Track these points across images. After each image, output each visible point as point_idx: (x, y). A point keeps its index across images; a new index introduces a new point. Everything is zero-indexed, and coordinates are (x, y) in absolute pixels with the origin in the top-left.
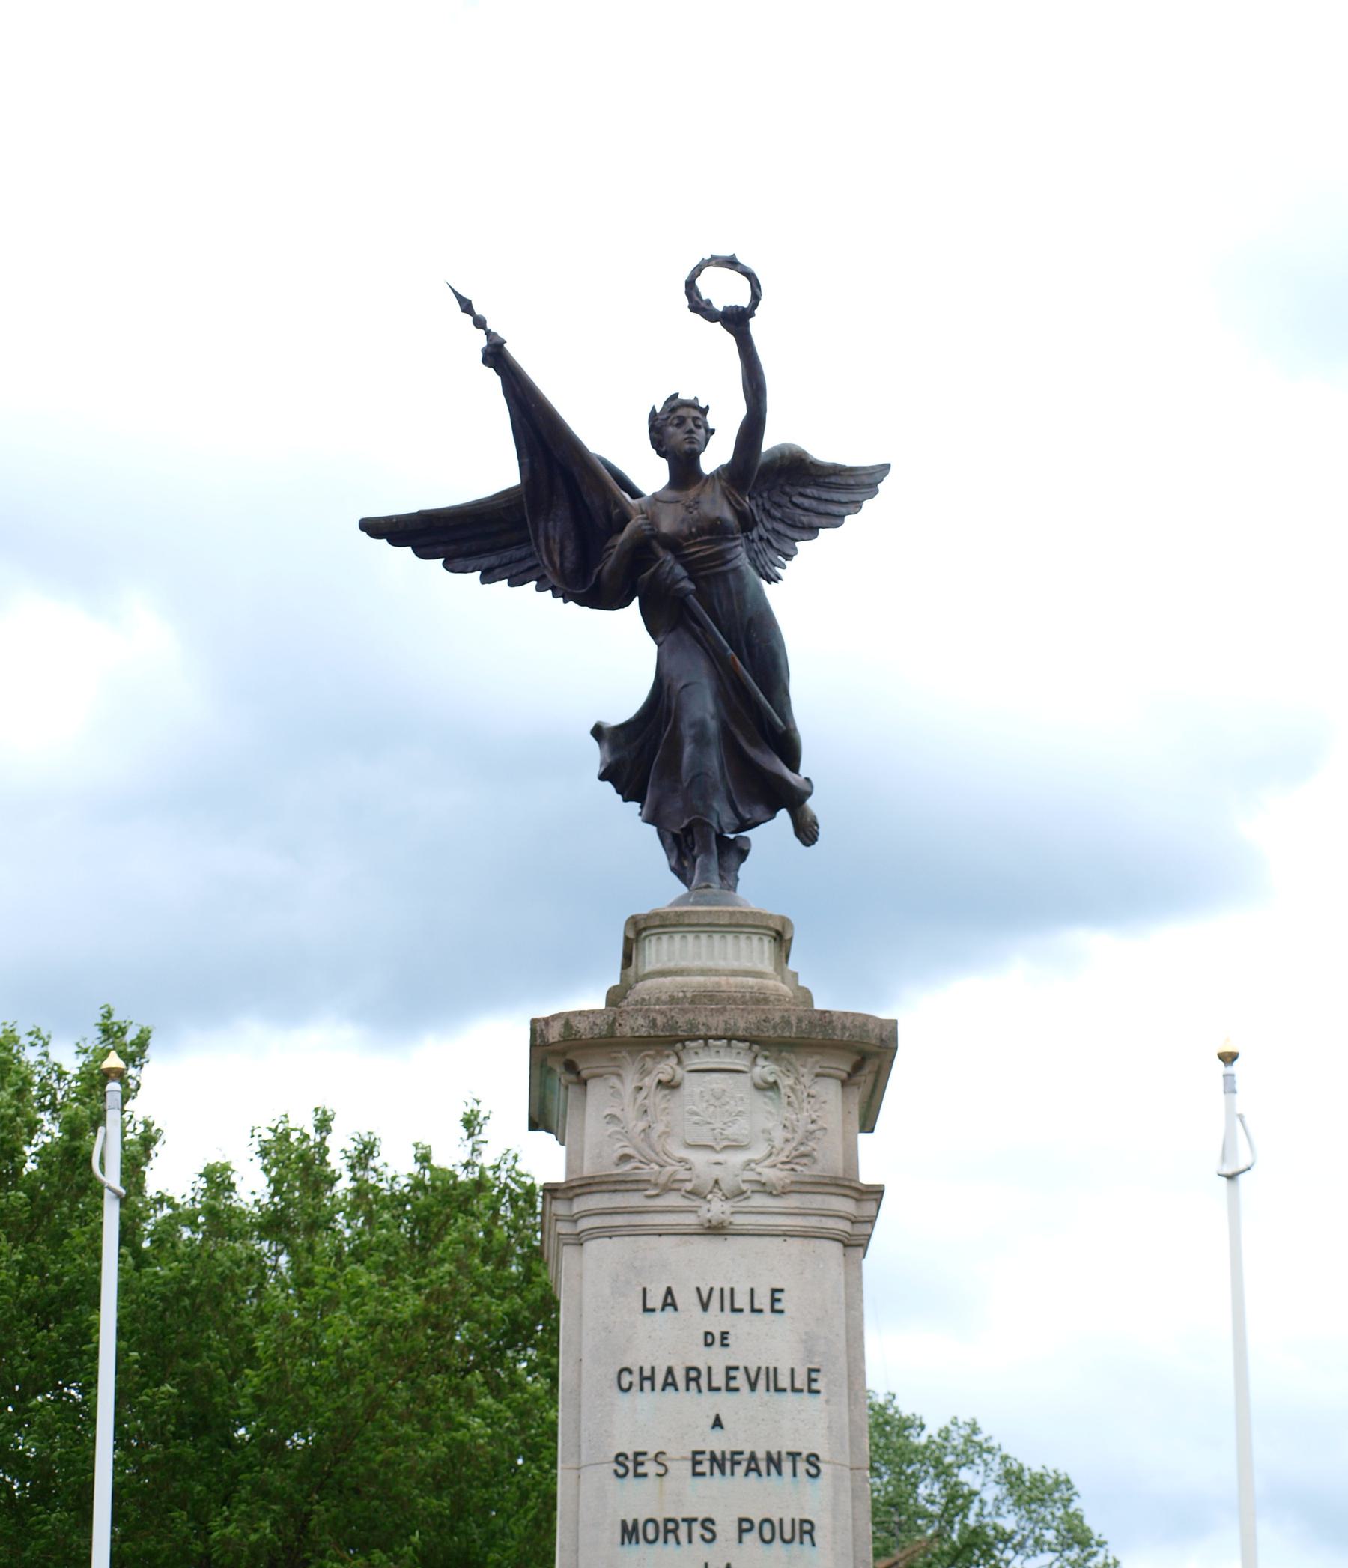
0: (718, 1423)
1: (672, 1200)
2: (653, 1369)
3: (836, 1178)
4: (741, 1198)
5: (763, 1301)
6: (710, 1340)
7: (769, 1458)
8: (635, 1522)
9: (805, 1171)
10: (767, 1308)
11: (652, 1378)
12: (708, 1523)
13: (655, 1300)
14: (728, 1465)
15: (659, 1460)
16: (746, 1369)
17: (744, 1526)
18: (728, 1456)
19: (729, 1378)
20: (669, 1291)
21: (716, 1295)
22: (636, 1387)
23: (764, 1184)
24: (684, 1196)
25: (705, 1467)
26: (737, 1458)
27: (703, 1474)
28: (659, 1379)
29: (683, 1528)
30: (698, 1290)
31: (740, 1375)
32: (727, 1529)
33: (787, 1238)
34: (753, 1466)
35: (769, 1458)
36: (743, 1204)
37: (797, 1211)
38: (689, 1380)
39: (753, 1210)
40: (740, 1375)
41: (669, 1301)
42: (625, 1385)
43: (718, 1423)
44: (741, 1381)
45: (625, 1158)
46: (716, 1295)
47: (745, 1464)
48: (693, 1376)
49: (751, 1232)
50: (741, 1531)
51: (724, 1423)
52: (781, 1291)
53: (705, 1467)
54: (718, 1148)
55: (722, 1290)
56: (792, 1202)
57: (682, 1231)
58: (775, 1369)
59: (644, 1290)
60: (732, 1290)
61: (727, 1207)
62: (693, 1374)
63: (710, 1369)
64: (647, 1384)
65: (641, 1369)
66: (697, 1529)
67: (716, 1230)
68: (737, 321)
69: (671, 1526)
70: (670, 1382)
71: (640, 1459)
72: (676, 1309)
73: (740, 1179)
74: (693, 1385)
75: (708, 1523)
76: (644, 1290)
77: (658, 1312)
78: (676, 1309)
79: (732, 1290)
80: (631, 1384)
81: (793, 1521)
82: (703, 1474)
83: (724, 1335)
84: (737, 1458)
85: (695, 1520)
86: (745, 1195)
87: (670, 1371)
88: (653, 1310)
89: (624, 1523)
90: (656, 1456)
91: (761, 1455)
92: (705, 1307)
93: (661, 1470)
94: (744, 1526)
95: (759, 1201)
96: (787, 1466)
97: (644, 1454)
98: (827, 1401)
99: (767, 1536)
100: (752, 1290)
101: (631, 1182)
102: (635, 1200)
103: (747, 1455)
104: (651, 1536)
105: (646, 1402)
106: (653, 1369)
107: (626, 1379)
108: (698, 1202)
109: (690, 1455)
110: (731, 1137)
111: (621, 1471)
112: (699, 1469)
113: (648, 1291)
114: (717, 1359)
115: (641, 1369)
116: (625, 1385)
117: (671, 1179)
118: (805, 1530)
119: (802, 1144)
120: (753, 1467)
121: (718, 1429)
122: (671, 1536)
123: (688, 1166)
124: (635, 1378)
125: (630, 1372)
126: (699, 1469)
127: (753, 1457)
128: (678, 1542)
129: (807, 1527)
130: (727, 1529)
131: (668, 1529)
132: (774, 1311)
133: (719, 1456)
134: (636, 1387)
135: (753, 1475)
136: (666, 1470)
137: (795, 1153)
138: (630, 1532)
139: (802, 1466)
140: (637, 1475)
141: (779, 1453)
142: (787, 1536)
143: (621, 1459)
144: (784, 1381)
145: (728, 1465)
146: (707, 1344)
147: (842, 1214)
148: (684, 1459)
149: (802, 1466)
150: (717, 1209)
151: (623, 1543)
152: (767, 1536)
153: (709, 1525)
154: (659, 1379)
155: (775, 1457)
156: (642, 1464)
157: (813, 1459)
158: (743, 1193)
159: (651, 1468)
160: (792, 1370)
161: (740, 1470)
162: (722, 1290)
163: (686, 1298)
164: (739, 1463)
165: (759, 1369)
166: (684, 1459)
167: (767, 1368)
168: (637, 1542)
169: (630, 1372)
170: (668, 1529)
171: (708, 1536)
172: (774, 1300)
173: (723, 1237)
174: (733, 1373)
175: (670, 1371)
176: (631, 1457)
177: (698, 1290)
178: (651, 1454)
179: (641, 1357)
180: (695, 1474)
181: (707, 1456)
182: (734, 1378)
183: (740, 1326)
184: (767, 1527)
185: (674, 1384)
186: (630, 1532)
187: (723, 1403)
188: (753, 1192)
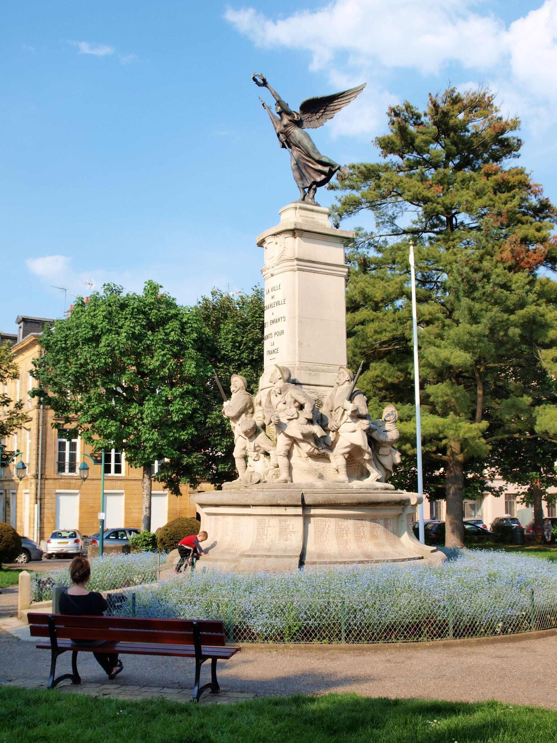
1: (267, 271)
9: (282, 258)
32: (273, 335)
61: (272, 270)
67: (272, 275)
68: (265, 83)
95: (276, 267)
114: (272, 301)
118: (282, 332)
130: (273, 335)
139: (283, 319)
149: (283, 319)
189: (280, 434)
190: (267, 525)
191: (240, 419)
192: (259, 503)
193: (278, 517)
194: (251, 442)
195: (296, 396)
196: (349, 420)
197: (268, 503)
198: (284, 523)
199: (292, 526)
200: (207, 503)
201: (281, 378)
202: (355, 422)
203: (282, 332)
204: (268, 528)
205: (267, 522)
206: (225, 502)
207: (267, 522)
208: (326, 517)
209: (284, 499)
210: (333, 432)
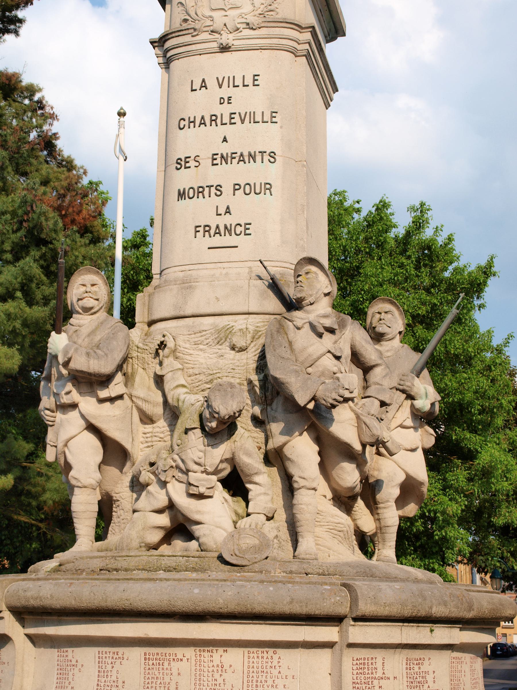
0: (225, 140)
1: (204, 36)
2: (195, 117)
3: (285, 19)
4: (238, 31)
5: (249, 81)
6: (222, 101)
7: (250, 155)
8: (184, 189)
10: (251, 84)
11: (194, 122)
12: (219, 187)
13: (196, 86)
14: (229, 159)
15: (196, 159)
16: (240, 114)
17: (236, 187)
18: (229, 155)
19: (232, 118)
20: (204, 81)
21: (226, 80)
22: (187, 127)
23: (248, 24)
24: (210, 34)
25: (218, 161)
26: (234, 155)
27: (217, 164)
28: (197, 123)
29: (207, 190)
30: (217, 78)
31: (237, 116)
32: (227, 189)
33: (262, 51)
34: (242, 159)
35: (250, 155)
36: (239, 34)
37: (266, 36)
38: (212, 121)
39: (244, 37)
40: (237, 116)
41: (204, 85)
42: (182, 127)
43: (225, 140)
44: (237, 119)
45: (185, 20)
46: (226, 80)
47: (237, 159)
48: (214, 119)
49: (244, 49)
50: (235, 190)
51: (228, 139)
52: (258, 75)
53: (218, 161)
54: (226, 9)
55: (229, 77)
56: (263, 32)
57: (210, 51)
58: (254, 113)
59: (192, 81)
60: (234, 77)
61: (231, 36)
62: (214, 118)
63: (222, 115)
64: (192, 125)
65: (189, 118)
66: (213, 189)
69: (201, 190)
70: (203, 123)
71: (187, 160)
72: (206, 89)
73: (236, 22)
74: (213, 123)
75: (219, 187)
76: (192, 81)
77: (198, 90)
78: (206, 89)
79: (234, 77)
80: (184, 126)
81: (261, 184)
82: (217, 164)
83: (229, 98)
84: (234, 155)
85: (213, 186)
86: (239, 30)
87: (203, 118)
88: (196, 90)
89: (179, 191)
90: (195, 158)
91: (246, 154)
92: (220, 86)
93: (197, 164)
94: (236, 187)
95: (248, 32)
96: (258, 158)
97: (189, 157)
98: (281, 127)
99: (248, 191)
100: (244, 76)
101: (185, 30)
102: (187, 39)
103: (239, 154)
104: (191, 196)
105: (190, 133)
106: (195, 117)
107: (182, 123)
108: (217, 36)
109: (211, 156)
110: (233, 3)
111: (179, 166)
112: (215, 162)
113: (194, 82)
114: (226, 110)
115: (189, 118)
116: (182, 127)
117: (204, 25)
118: (268, 187)
119: (270, 5)
120: (242, 159)
121: (225, 142)
122: (200, 194)
123: (212, 19)
124: (186, 123)
125: (184, 120)
126: (215, 162)
127: (242, 155)
128: (204, 198)
129: (268, 186)
131: (200, 191)
132: (254, 85)
133: (225, 155)
134: (187, 127)
135: (242, 163)
136: (200, 164)
137: (265, 10)
138: (181, 195)
139: (266, 157)
140: (186, 168)
141: (255, 152)
142: (258, 191)
143: (179, 161)
144: (258, 118)
145: (229, 159)
146: (221, 104)
147: (290, 37)
148: (209, 158)
149: (266, 157)
150: (227, 38)
151: (178, 200)
152: (248, 191)
153: (218, 188)
154: (197, 123)
155: (253, 154)
156: (188, 162)
157: (272, 155)
158: (238, 29)
159: (192, 164)
160: (263, 113)
161: (235, 161)
162: (229, 77)
163: (211, 83)
164: (235, 158)
165: (246, 113)
166: (209, 158)
167: (250, 113)
168: (185, 199)
169: (184, 120)
170: (200, 191)
171: (218, 193)
172: (255, 80)
173: (230, 53)
174: (233, 116)
175: (203, 118)
176: (183, 160)
177: (217, 78)
178: (192, 158)
179: (190, 113)
180: (213, 165)
181: (219, 156)
182: (234, 118)
183: (236, 93)
184: (247, 187)
185: (204, 124)
186: (181, 195)
187: (228, 130)
188: (243, 29)
189: (301, 434)
190: (379, 674)
191: (111, 386)
192: (385, 612)
193: (406, 651)
194: (213, 446)
195: (364, 343)
196: (409, 422)
197: (407, 612)
198: (416, 668)
199: (431, 675)
200: (225, 610)
201: (326, 295)
202: (415, 429)
203: (268, 187)
204: (383, 682)
205: (379, 665)
206: (259, 608)
207: (379, 665)
208: (464, 652)
209: (445, 604)
210: (372, 445)
